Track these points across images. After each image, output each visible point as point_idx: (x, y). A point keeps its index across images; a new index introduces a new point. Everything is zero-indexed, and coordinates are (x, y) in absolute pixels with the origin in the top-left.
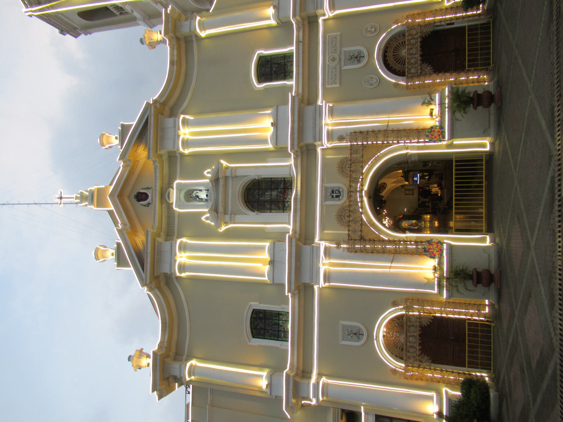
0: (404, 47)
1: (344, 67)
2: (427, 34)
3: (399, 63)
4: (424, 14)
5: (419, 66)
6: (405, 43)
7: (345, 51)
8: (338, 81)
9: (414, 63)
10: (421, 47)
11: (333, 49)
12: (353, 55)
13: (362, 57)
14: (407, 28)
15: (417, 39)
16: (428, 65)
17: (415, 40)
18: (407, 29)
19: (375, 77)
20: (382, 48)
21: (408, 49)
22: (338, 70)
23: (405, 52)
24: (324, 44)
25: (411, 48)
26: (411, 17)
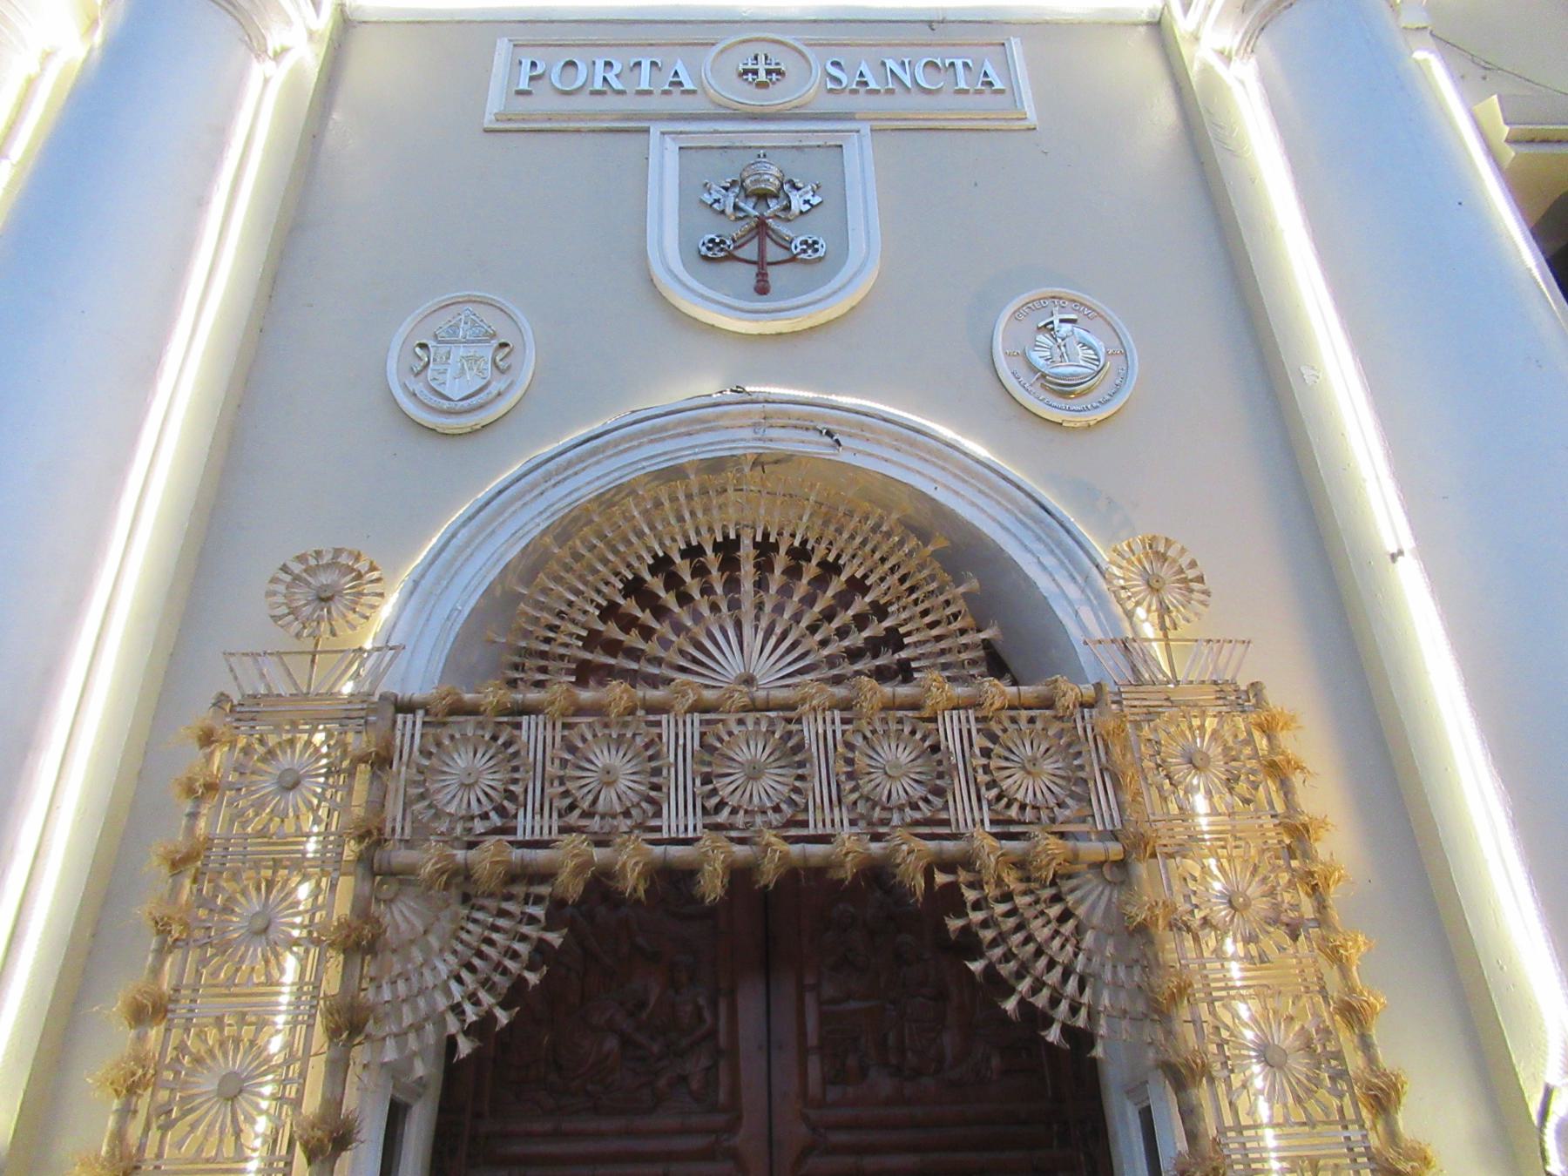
0: (831, 661)
1: (672, 146)
2: (1006, 969)
3: (610, 612)
4: (1308, 908)
5: (516, 854)
6: (881, 675)
7: (841, 146)
8: (544, 102)
9: (584, 786)
10: (797, 877)
11: (864, 68)
12: (788, 208)
13: (762, 276)
14: (1088, 691)
15: (935, 826)
16: (515, 994)
17: (918, 792)
18: (1070, 692)
19: (494, 389)
20: (844, 457)
21: (793, 708)
22: (656, 104)
23: (749, 680)
24: (930, 23)
25: (799, 747)
26: (1249, 741)
